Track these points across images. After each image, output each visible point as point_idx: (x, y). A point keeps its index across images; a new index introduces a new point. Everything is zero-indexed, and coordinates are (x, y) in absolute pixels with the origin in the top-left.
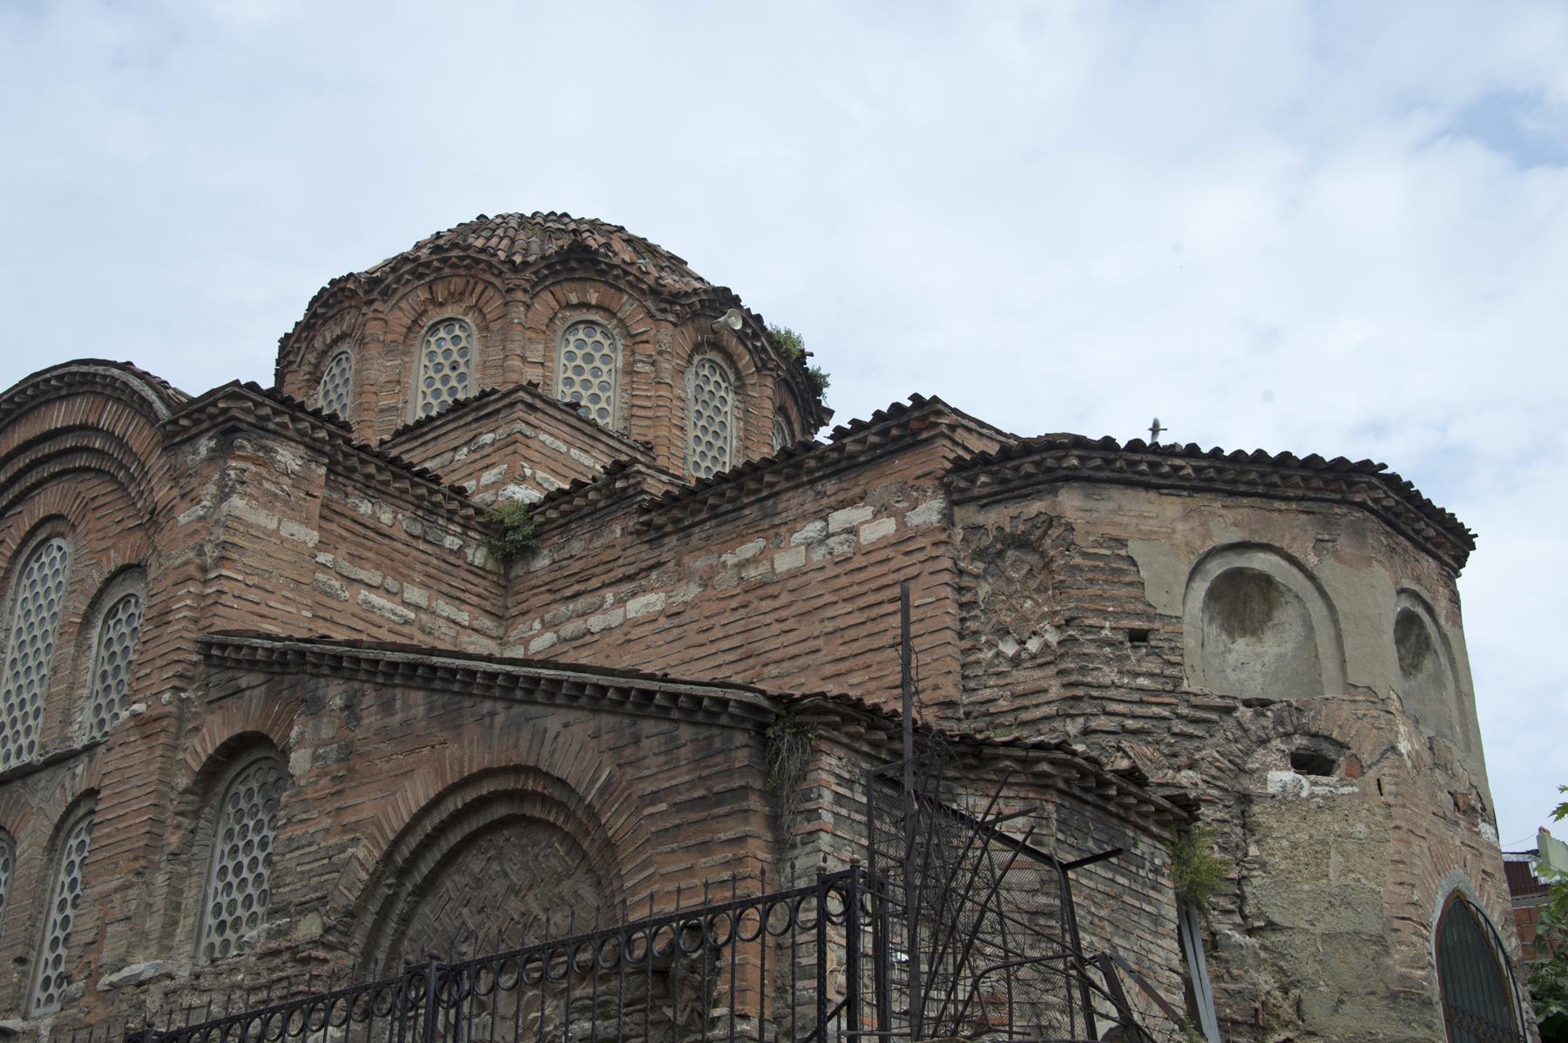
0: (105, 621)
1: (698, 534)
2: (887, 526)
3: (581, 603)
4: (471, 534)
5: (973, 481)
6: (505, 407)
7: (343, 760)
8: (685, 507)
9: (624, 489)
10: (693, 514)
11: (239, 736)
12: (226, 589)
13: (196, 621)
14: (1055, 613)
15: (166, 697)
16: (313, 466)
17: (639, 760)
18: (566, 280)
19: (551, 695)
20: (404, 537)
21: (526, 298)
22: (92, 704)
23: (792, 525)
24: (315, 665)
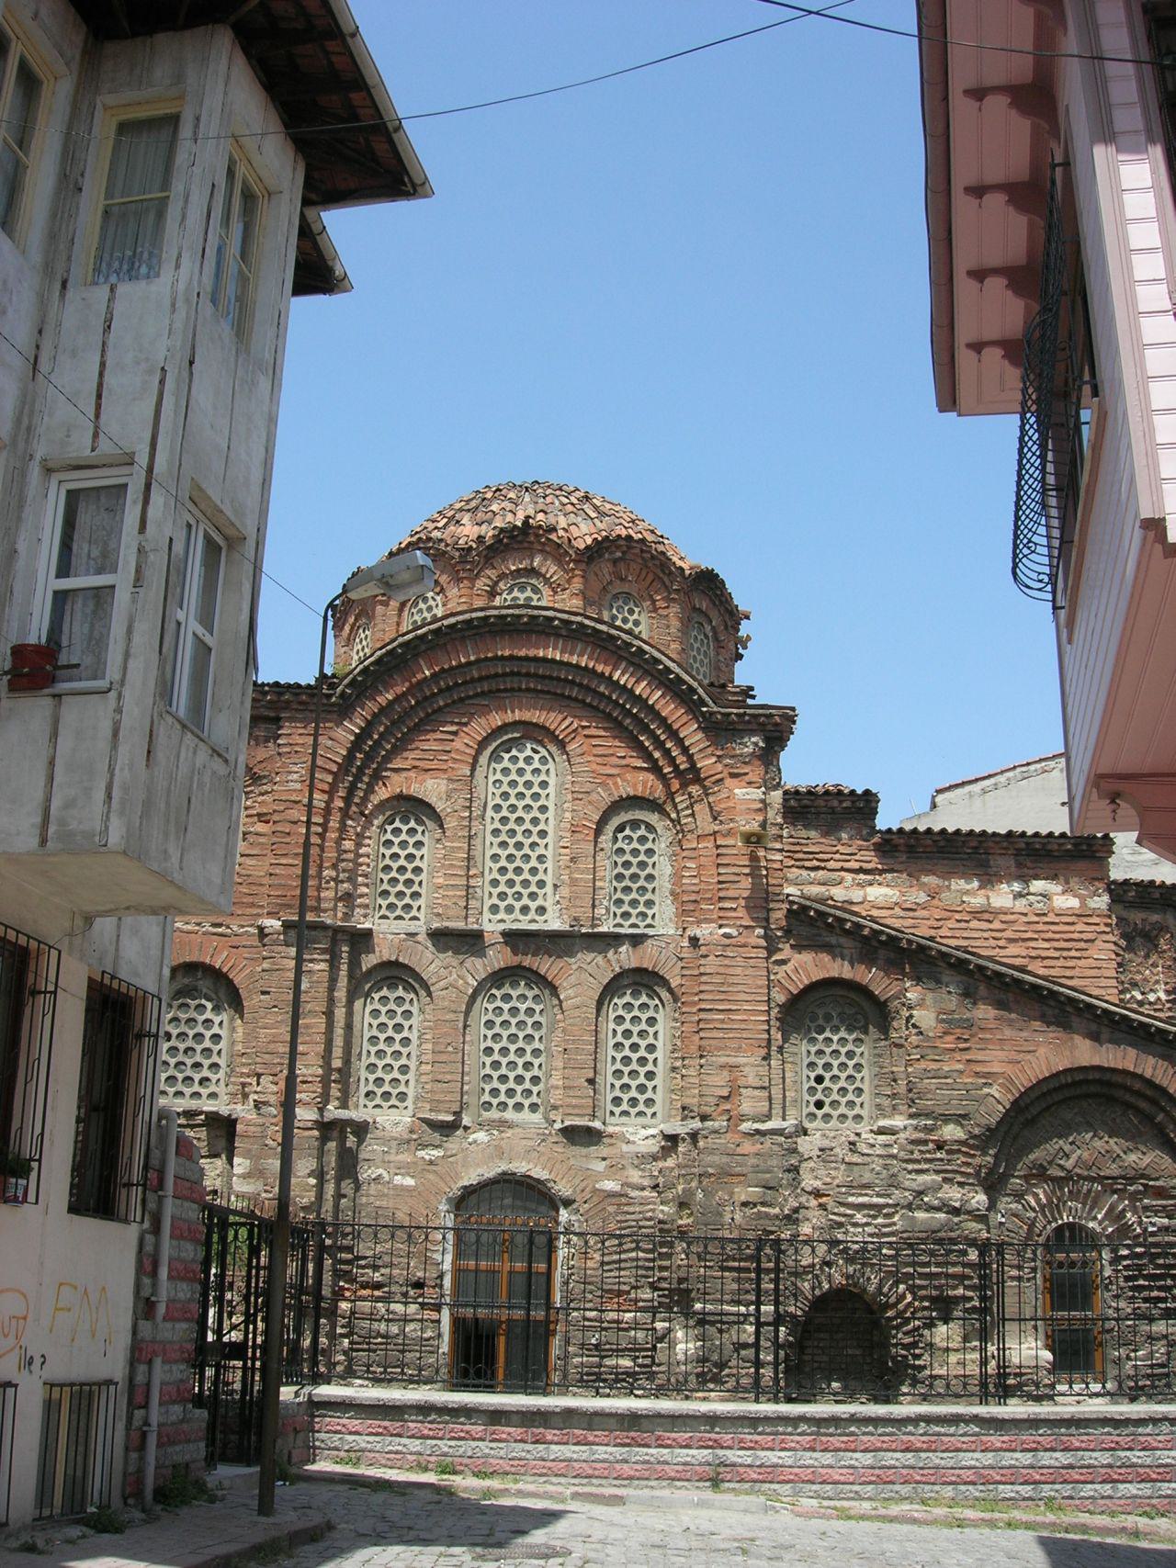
2: (1073, 902)
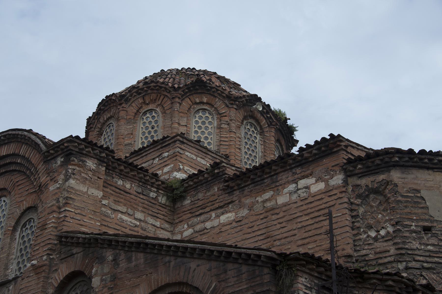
0: (22, 229)
1: (247, 190)
2: (321, 186)
3: (202, 218)
4: (160, 191)
5: (355, 167)
6: (172, 142)
7: (112, 281)
8: (242, 179)
9: (218, 173)
10: (245, 182)
11: (73, 272)
12: (68, 215)
13: (56, 228)
14: (391, 220)
15: (45, 258)
16: (100, 167)
17: (226, 279)
18: (195, 93)
19: (192, 254)
20: (135, 193)
21: (180, 101)
22: (16, 261)
23: (284, 186)
24: (101, 244)
